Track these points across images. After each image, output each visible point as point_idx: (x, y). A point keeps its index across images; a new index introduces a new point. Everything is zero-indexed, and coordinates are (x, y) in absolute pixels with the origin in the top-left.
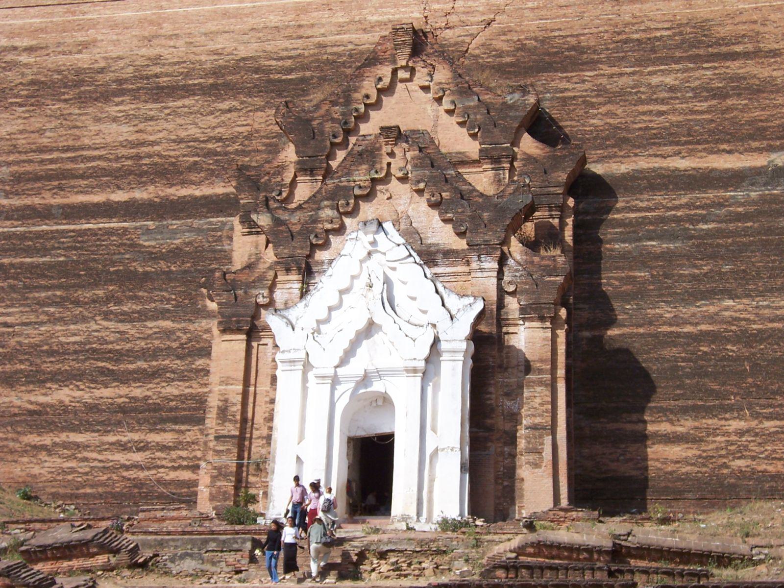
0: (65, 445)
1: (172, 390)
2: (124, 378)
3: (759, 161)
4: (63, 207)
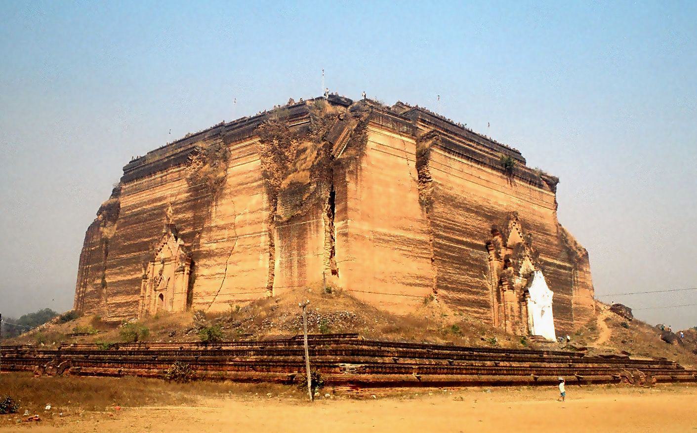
0: (466, 310)
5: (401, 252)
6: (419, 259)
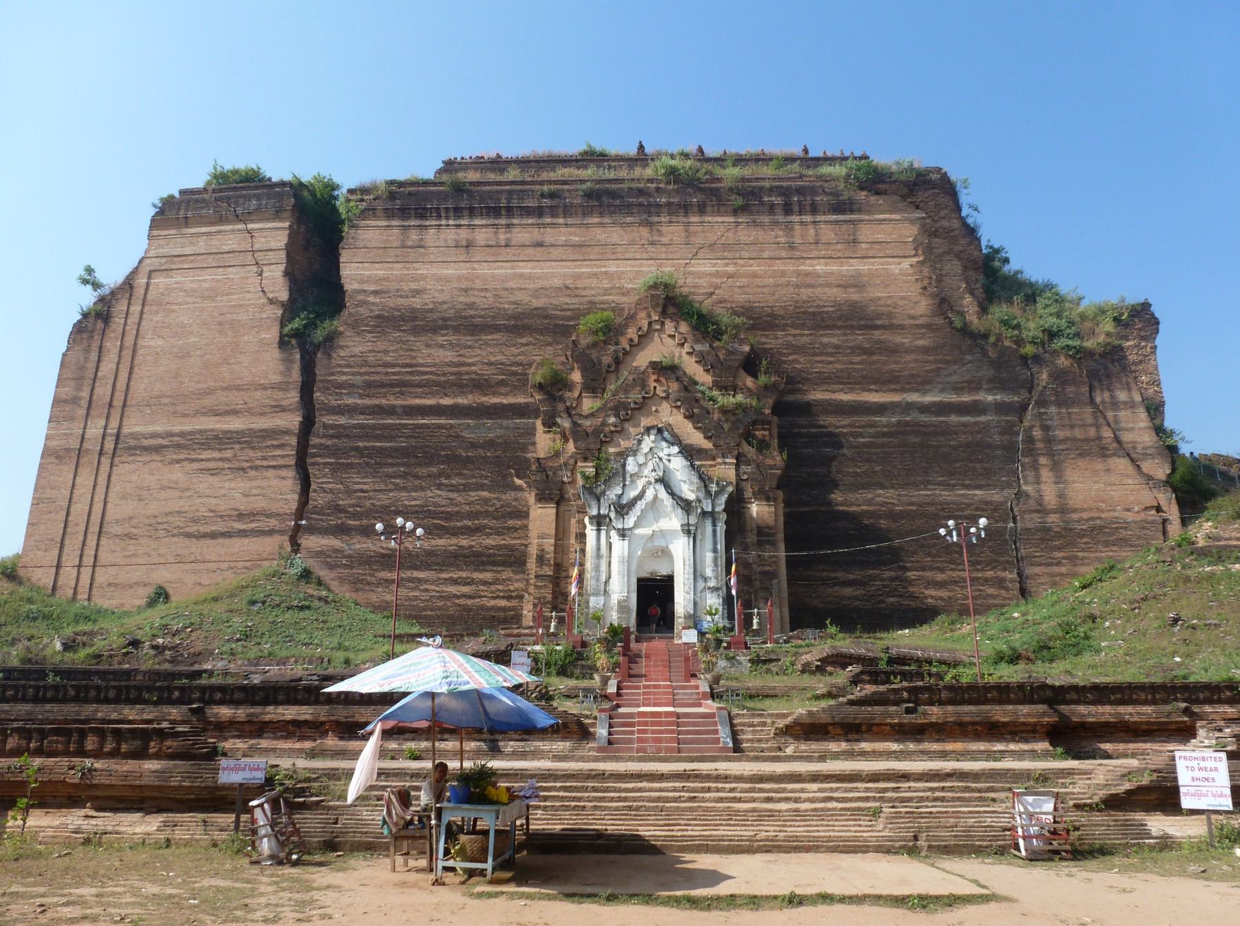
0: (410, 580)
1: (489, 542)
2: (455, 532)
3: (896, 398)
4: (404, 407)
5: (196, 465)
6: (252, 473)
